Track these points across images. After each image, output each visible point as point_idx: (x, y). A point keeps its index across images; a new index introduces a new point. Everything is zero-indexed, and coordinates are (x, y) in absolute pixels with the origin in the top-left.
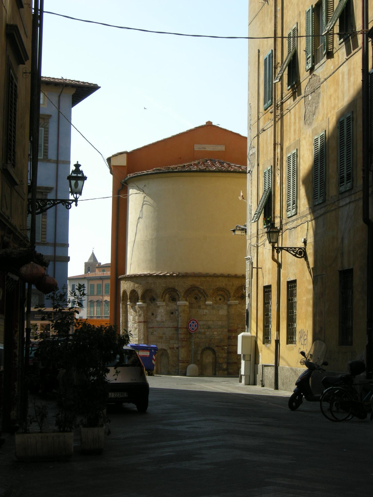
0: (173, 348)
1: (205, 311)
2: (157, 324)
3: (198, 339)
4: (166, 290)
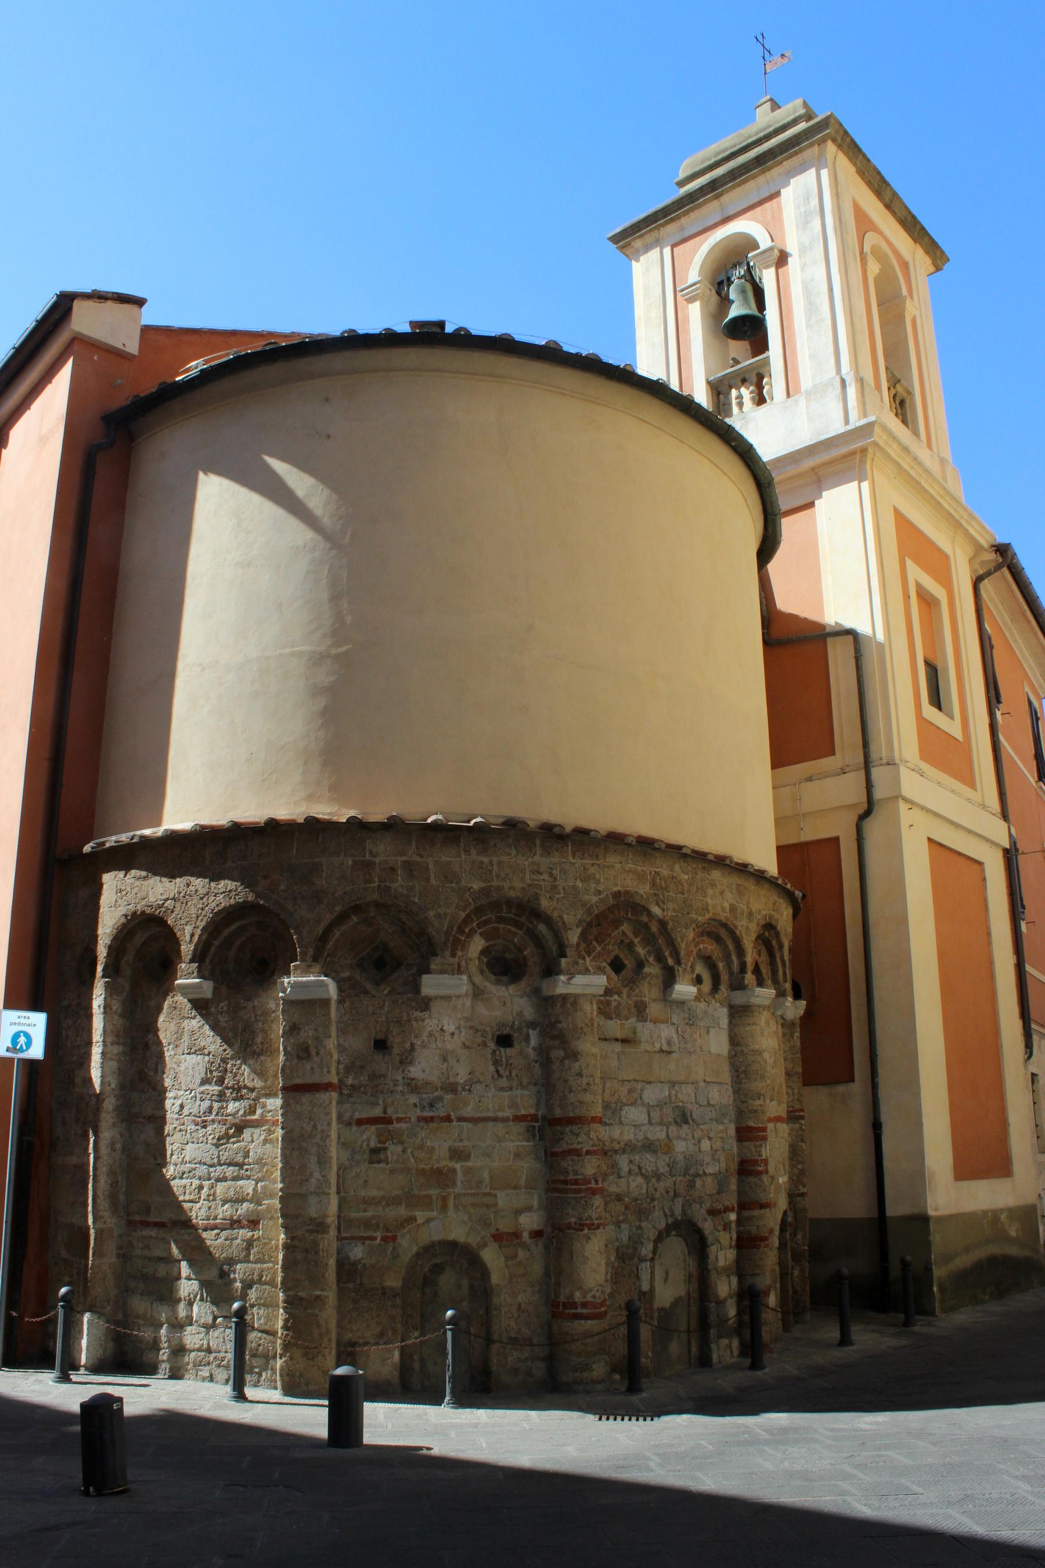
0: (517, 1235)
1: (666, 1032)
2: (413, 1099)
3: (640, 1180)
4: (479, 911)
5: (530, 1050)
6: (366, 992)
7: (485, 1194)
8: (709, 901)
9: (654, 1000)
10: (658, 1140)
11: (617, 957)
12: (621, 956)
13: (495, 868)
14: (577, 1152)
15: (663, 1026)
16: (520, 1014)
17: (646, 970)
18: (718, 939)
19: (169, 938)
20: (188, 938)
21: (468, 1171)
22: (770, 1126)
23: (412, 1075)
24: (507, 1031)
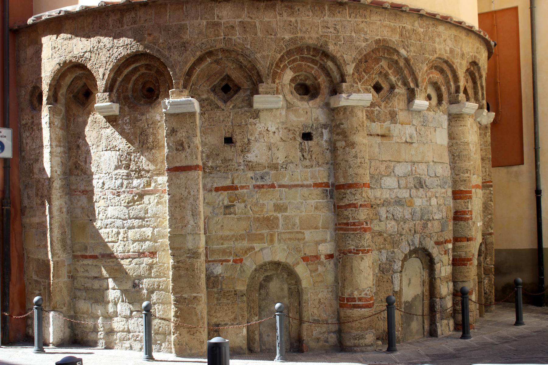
0: (317, 257)
1: (409, 130)
2: (250, 174)
3: (393, 223)
4: (289, 53)
5: (323, 142)
6: (218, 107)
7: (297, 232)
8: (437, 46)
9: (401, 110)
10: (405, 198)
11: (377, 83)
12: (380, 82)
13: (299, 25)
14: (355, 206)
15: (407, 127)
16: (317, 119)
17: (396, 90)
18: (442, 71)
19: (89, 76)
20: (101, 77)
21: (286, 218)
22: (473, 190)
23: (249, 159)
24: (308, 130)
